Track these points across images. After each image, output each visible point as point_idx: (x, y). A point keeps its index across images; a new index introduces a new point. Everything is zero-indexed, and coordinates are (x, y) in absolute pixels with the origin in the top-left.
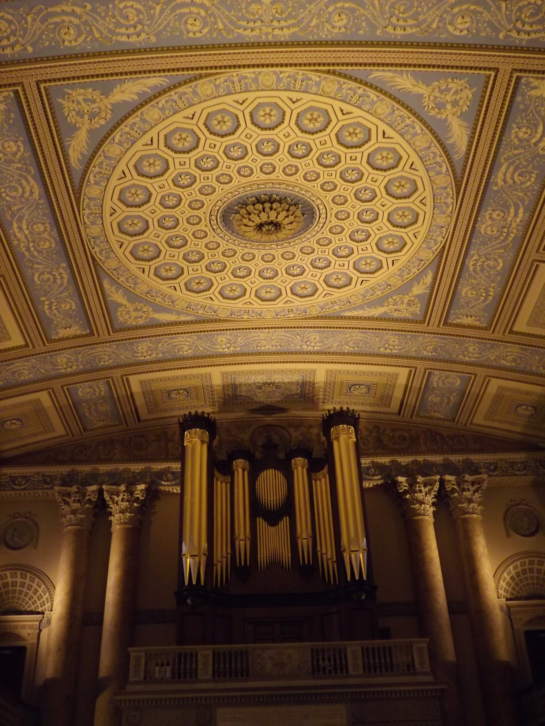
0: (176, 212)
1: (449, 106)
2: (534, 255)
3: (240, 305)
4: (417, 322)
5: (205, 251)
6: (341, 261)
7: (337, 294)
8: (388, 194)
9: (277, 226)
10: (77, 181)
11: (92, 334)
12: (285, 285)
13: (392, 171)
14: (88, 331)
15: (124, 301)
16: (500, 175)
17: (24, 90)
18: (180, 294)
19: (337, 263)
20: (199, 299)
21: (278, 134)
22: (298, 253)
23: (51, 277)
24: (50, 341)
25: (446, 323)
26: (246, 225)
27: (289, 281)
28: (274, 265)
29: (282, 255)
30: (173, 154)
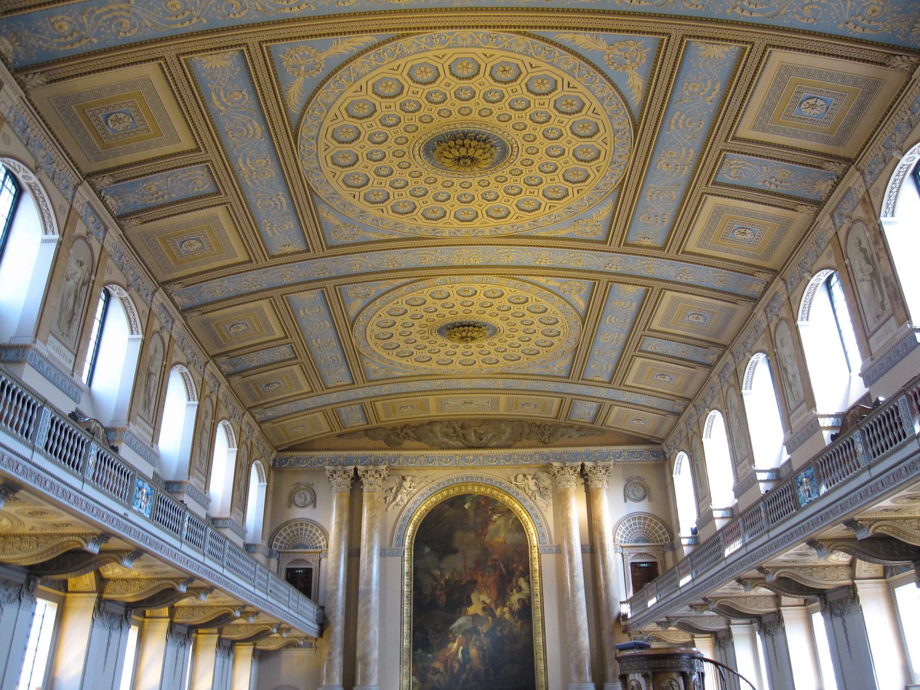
0: (384, 147)
1: (628, 62)
2: (703, 189)
3: (441, 225)
4: (600, 242)
5: (409, 179)
6: (532, 189)
7: (528, 216)
8: (573, 133)
9: (473, 159)
10: (294, 122)
11: (308, 250)
12: (481, 208)
13: (576, 115)
14: (304, 248)
15: (337, 223)
16: (673, 121)
17: (248, 49)
18: (387, 216)
19: (528, 191)
20: (405, 219)
21: (474, 84)
22: (492, 181)
23: (273, 203)
24: (273, 257)
25: (626, 244)
26: (446, 158)
27: (484, 205)
28: (471, 191)
29: (479, 183)
30: (379, 99)
